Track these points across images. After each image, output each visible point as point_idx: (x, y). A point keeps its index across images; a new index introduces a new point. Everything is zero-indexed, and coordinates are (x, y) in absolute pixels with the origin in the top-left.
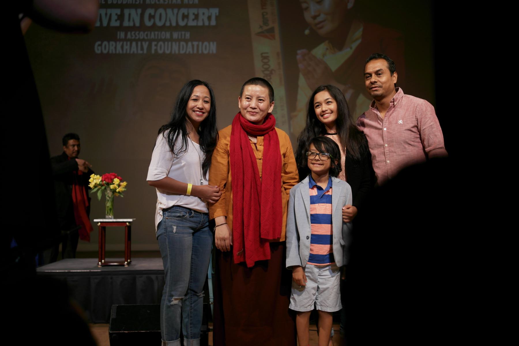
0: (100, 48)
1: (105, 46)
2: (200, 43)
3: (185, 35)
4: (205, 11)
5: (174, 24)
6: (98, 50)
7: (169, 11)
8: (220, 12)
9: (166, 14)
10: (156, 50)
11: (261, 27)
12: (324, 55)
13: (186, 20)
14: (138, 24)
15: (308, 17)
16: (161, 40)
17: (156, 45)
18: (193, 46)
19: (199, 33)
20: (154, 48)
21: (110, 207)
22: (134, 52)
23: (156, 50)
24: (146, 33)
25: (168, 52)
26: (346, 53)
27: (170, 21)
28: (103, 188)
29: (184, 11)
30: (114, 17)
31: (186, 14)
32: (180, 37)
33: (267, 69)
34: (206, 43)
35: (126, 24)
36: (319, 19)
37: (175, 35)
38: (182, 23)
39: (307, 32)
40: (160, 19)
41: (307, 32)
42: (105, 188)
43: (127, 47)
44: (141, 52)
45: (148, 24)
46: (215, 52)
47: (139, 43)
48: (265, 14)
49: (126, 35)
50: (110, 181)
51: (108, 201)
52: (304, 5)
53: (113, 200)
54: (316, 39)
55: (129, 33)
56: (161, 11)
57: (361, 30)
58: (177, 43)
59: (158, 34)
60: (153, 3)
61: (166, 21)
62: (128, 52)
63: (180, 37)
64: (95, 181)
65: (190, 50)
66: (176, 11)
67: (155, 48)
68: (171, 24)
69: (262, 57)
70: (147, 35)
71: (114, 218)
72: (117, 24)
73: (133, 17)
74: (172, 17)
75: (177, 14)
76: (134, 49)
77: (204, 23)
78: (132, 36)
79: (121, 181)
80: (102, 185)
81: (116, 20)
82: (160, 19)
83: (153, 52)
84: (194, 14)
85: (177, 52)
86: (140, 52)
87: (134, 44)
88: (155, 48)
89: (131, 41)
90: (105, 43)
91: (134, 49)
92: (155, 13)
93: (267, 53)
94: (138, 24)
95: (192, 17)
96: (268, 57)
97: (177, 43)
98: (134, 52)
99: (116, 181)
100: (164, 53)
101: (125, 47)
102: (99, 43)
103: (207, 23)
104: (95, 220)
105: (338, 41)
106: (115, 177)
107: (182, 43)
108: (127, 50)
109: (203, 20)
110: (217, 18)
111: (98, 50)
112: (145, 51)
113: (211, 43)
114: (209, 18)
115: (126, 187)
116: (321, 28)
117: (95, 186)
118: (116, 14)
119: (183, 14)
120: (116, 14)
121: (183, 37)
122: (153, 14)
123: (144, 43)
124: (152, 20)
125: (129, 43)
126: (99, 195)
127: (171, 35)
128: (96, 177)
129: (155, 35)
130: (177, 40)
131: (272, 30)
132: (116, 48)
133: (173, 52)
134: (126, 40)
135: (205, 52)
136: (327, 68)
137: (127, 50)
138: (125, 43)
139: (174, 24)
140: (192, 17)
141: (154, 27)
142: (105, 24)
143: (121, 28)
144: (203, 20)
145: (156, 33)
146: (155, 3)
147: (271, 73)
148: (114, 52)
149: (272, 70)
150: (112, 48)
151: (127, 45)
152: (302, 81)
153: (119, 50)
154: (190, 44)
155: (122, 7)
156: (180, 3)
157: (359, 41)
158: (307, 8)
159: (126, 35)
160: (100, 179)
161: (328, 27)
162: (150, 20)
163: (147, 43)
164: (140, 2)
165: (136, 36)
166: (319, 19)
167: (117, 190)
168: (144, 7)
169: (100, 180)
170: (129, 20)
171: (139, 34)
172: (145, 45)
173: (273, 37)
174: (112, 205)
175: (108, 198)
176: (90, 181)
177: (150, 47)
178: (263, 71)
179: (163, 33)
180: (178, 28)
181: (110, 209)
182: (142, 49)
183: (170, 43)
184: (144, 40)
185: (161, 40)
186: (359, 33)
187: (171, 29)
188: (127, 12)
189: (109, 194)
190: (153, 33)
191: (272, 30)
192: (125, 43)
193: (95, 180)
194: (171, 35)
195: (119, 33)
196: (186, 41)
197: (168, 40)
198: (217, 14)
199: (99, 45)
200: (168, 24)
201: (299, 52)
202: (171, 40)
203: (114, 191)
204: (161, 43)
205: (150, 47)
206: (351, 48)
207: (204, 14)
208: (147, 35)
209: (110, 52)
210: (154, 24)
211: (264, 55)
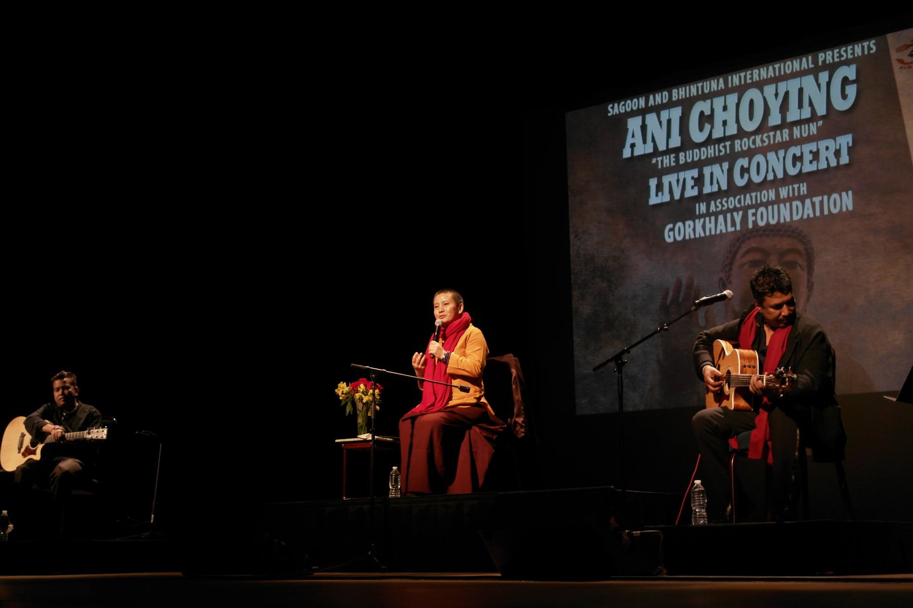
0: (671, 233)
2: (826, 197)
3: (799, 188)
4: (830, 142)
5: (780, 175)
7: (771, 156)
10: (755, 222)
13: (798, 164)
14: (724, 187)
16: (762, 204)
17: (754, 215)
18: (813, 204)
19: (821, 182)
20: (751, 219)
23: (755, 222)
24: (738, 197)
27: (773, 171)
29: (795, 150)
30: (690, 183)
31: (798, 154)
32: (791, 195)
34: (835, 196)
35: (707, 189)
37: (783, 192)
38: (792, 171)
40: (758, 173)
43: (710, 225)
44: (733, 229)
45: (740, 182)
46: (851, 208)
47: (729, 215)
55: (713, 203)
56: (759, 158)
58: (788, 204)
60: (745, 148)
61: (767, 172)
62: (713, 233)
63: (791, 195)
65: (809, 212)
66: (781, 153)
67: (754, 218)
72: (695, 192)
73: (718, 175)
76: (721, 227)
77: (828, 163)
78: (717, 207)
81: (692, 188)
82: (758, 173)
83: (750, 226)
84: (811, 152)
85: (788, 220)
86: (731, 229)
87: (721, 218)
88: (754, 218)
89: (716, 214)
90: (680, 224)
91: (722, 226)
95: (808, 157)
97: (788, 204)
100: (768, 224)
101: (708, 226)
102: (671, 226)
103: (833, 163)
104: (337, 441)
107: (795, 203)
112: (738, 228)
113: (844, 194)
114: (837, 153)
118: (693, 178)
119: (794, 155)
120: (693, 178)
121: (796, 194)
122: (746, 166)
123: (735, 214)
124: (746, 176)
125: (713, 218)
126: (349, 409)
127: (777, 194)
129: (751, 197)
130: (784, 201)
132: (694, 230)
133: (782, 221)
134: (708, 214)
135: (835, 211)
138: (707, 219)
141: (750, 187)
142: (677, 196)
143: (700, 198)
145: (753, 194)
150: (689, 231)
153: (700, 232)
154: (808, 202)
155: (699, 165)
162: (742, 177)
163: (741, 213)
165: (723, 206)
168: (732, 157)
171: (727, 202)
172: (738, 217)
177: (745, 219)
179: (765, 192)
182: (734, 224)
183: (776, 207)
184: (736, 209)
185: (762, 204)
187: (776, 183)
188: (707, 171)
190: (748, 196)
192: (707, 219)
193: (343, 388)
194: (777, 194)
196: (802, 199)
197: (772, 203)
198: (850, 144)
199: (670, 230)
200: (770, 177)
202: (778, 201)
204: (762, 209)
205: (745, 219)
207: (827, 148)
209: (687, 237)
210: (750, 179)
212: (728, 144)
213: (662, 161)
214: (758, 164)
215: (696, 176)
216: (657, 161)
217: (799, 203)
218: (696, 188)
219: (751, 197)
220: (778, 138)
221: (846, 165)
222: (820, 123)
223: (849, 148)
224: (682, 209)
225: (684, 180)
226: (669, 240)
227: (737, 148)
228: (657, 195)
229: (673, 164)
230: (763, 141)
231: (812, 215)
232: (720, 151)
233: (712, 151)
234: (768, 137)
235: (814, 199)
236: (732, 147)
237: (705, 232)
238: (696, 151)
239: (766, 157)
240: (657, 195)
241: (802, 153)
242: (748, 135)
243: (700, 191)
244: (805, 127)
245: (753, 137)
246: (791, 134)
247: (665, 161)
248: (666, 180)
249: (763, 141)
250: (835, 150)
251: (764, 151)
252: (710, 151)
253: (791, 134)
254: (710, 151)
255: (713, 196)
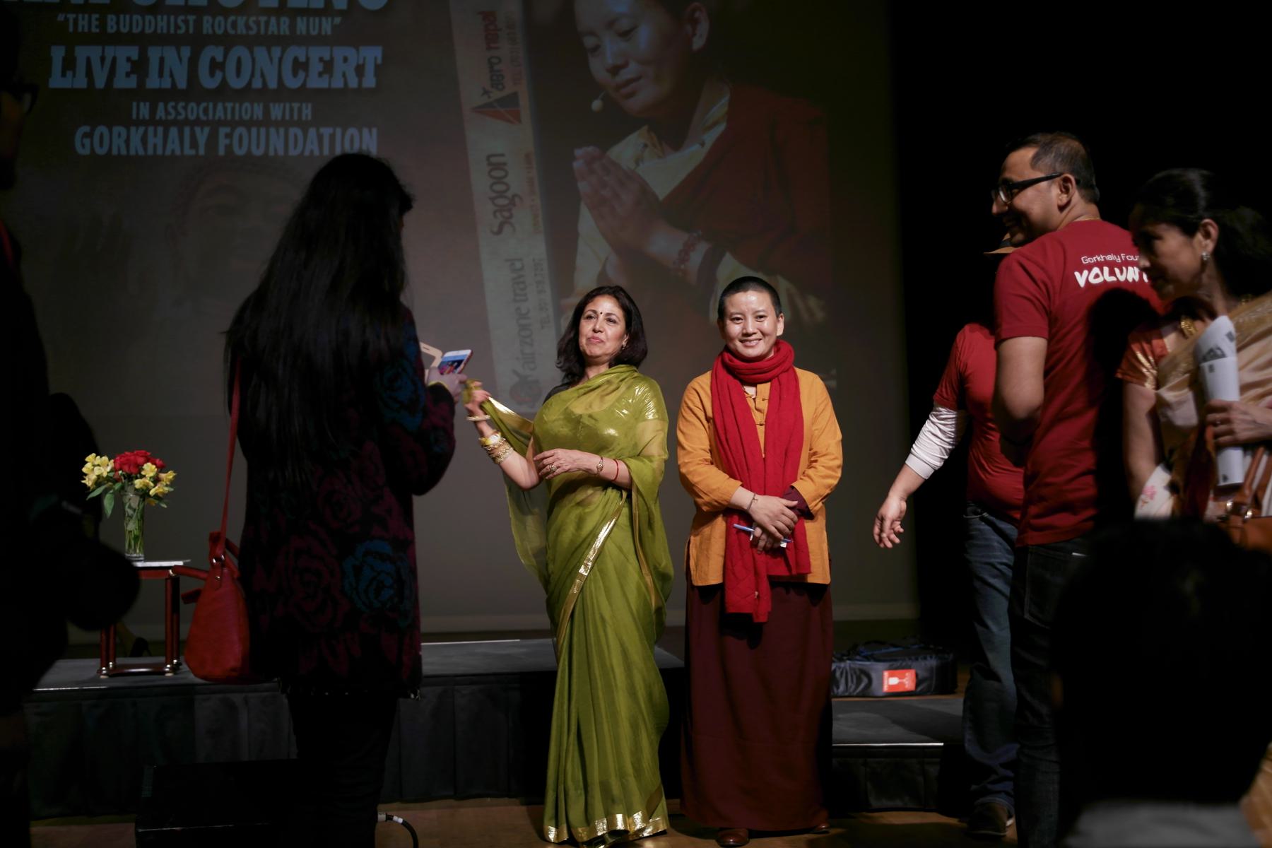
0: (87, 141)
1: (101, 136)
2: (339, 131)
3: (300, 110)
4: (350, 52)
5: (273, 85)
6: (83, 146)
7: (260, 52)
8: (384, 58)
9: (253, 60)
10: (229, 148)
11: (486, 92)
12: (638, 161)
13: (301, 74)
14: (182, 84)
15: (598, 68)
18: (320, 138)
20: (223, 142)
21: (136, 532)
22: (173, 151)
23: (229, 148)
24: (204, 105)
25: (258, 152)
26: (693, 155)
27: (263, 76)
28: (117, 486)
29: (298, 52)
30: (123, 67)
31: (302, 59)
32: (287, 117)
33: (501, 194)
35: (153, 82)
36: (625, 75)
37: (276, 111)
38: (292, 83)
39: (597, 105)
41: (597, 105)
42: (123, 488)
43: (155, 139)
44: (193, 152)
47: (187, 130)
48: (495, 61)
49: (153, 110)
50: (133, 470)
51: (131, 517)
52: (589, 42)
53: (142, 517)
54: (616, 124)
55: (161, 106)
56: (240, 51)
57: (725, 100)
59: (233, 109)
60: (220, 32)
61: (253, 75)
62: (160, 152)
63: (287, 117)
64: (97, 471)
66: (276, 52)
67: (227, 141)
68: (265, 83)
69: (490, 164)
70: (206, 111)
71: (146, 560)
72: (132, 83)
73: (171, 66)
74: (267, 67)
75: (280, 60)
76: (173, 146)
77: (346, 83)
78: (167, 113)
79: (162, 469)
80: (116, 481)
81: (128, 75)
83: (221, 152)
84: (321, 59)
85: (281, 152)
86: (189, 151)
87: (174, 131)
88: (227, 141)
89: (166, 125)
90: (102, 129)
92: (225, 57)
93: (502, 155)
94: (182, 84)
95: (316, 67)
96: (505, 164)
97: (282, 131)
98: (173, 151)
99: (149, 469)
101: (151, 141)
102: (86, 129)
103: (353, 83)
105: (670, 128)
106: (147, 461)
107: (293, 131)
108: (155, 146)
109: (344, 75)
110: (378, 69)
111: (82, 147)
112: (202, 152)
113: (365, 131)
114: (360, 70)
115: (172, 483)
116: (631, 95)
117: (99, 481)
118: (129, 59)
119: (296, 60)
120: (129, 59)
121: (296, 117)
122: (220, 59)
123: (198, 130)
124: (219, 75)
125: (160, 130)
126: (108, 504)
127: (267, 112)
128: (98, 460)
129: (225, 109)
130: (277, 124)
131: (512, 100)
134: (153, 122)
136: (645, 190)
137: (155, 146)
138: (151, 129)
139: (273, 85)
140: (316, 67)
141: (223, 92)
142: (100, 83)
143: (141, 93)
144: (344, 75)
145: (229, 105)
146: (226, 33)
147: (512, 203)
148: (124, 152)
149: (514, 196)
151: (155, 135)
152: (587, 222)
153: (136, 147)
154: (312, 132)
155: (142, 41)
156: (288, 33)
157: (721, 128)
158: (596, 48)
159: (153, 110)
160: (111, 464)
161: (646, 95)
162: (212, 74)
163: (207, 130)
164: (187, 30)
165: (178, 113)
166: (625, 75)
167: (152, 492)
168: (198, 41)
169: (109, 469)
170: (161, 75)
171: (185, 108)
172: (202, 135)
173: (517, 117)
174: (141, 528)
175: (130, 512)
176: (84, 470)
177: (213, 138)
178: (492, 199)
179: (247, 105)
180: (282, 93)
181: (136, 538)
182: (194, 144)
183: (263, 130)
184: (198, 122)
186: (720, 107)
187: (264, 95)
188: (154, 53)
189: (132, 500)
190: (220, 106)
191: (512, 100)
192: (151, 129)
193: (96, 467)
194: (267, 112)
195: (135, 104)
196: (304, 126)
197: (258, 124)
198: (379, 61)
199: (85, 135)
200: (257, 84)
201: (578, 152)
202: (267, 122)
203: (144, 494)
204: (241, 130)
205: (213, 138)
206: (703, 144)
207: (345, 60)
208: (206, 111)
209: (115, 152)
210: (224, 80)
211: (494, 160)
212: (191, 18)
213: (76, 21)
214: (239, 61)
215: (135, 57)
216: (67, 20)
217: (299, 133)
218: (134, 78)
219: (225, 109)
220: (273, 28)
221: (369, 90)
222: (338, 20)
223: (377, 67)
224: (107, 106)
225: (114, 60)
226: (87, 152)
227: (207, 29)
228: (64, 75)
229: (95, 30)
230: (248, 27)
231: (317, 153)
232: (177, 27)
233: (165, 24)
234: (258, 23)
235: (322, 130)
236: (198, 24)
237: (145, 149)
238: (136, 17)
239: (252, 53)
240: (64, 75)
241: (308, 59)
242: (226, 12)
243: (141, 82)
244: (315, 21)
245: (232, 18)
246: (293, 26)
247: (80, 23)
248: (81, 52)
249: (248, 27)
250: (357, 65)
251: (251, 42)
252: (162, 23)
253: (293, 26)
254: (162, 23)
255: (157, 96)
